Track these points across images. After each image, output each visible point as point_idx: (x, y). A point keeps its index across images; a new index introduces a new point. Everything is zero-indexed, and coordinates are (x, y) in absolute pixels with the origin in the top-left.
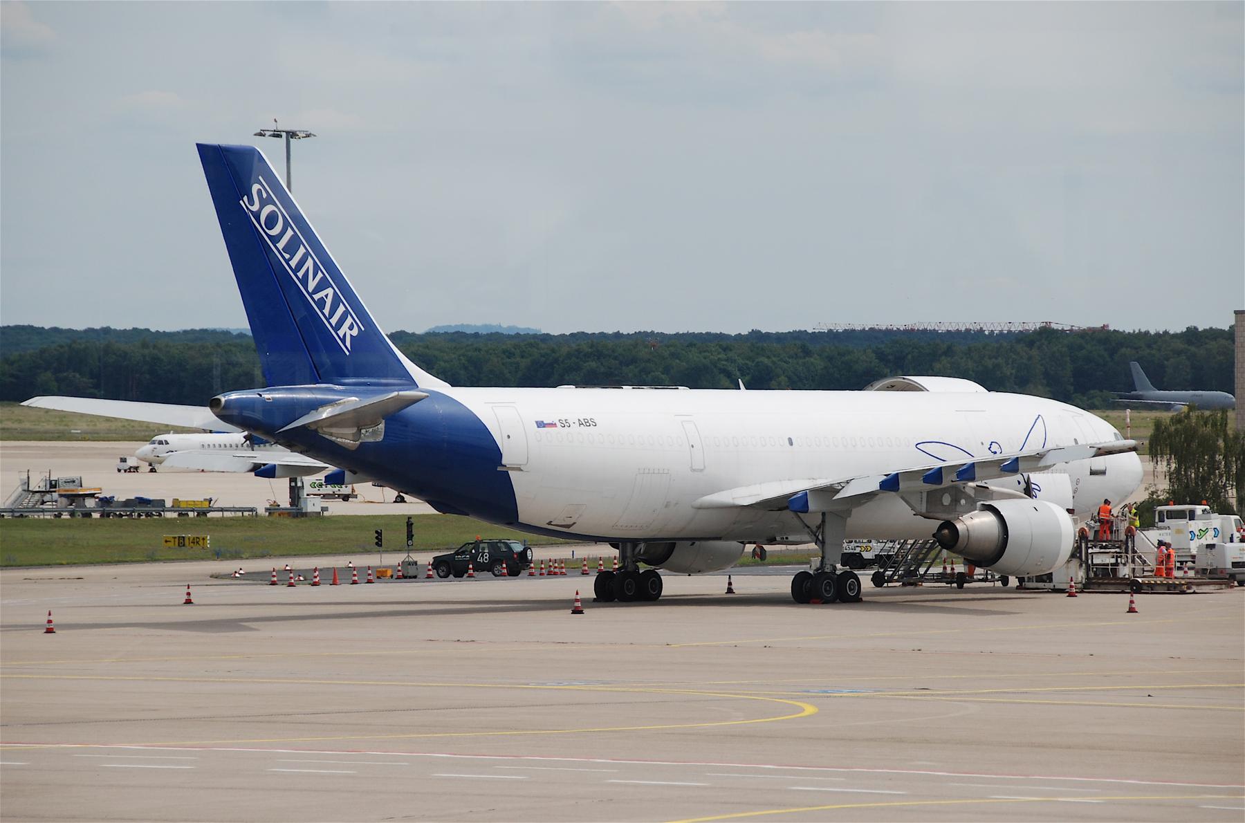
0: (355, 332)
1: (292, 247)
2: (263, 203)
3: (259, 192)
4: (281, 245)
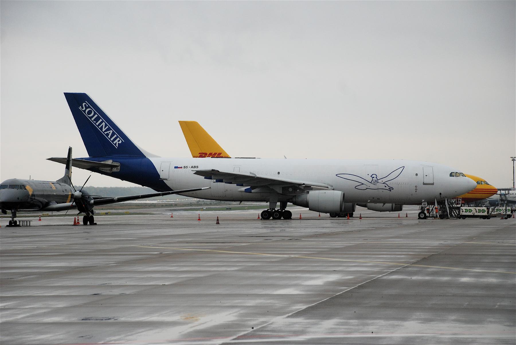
0: (120, 142)
1: (97, 120)
2: (86, 108)
3: (85, 105)
4: (93, 119)
